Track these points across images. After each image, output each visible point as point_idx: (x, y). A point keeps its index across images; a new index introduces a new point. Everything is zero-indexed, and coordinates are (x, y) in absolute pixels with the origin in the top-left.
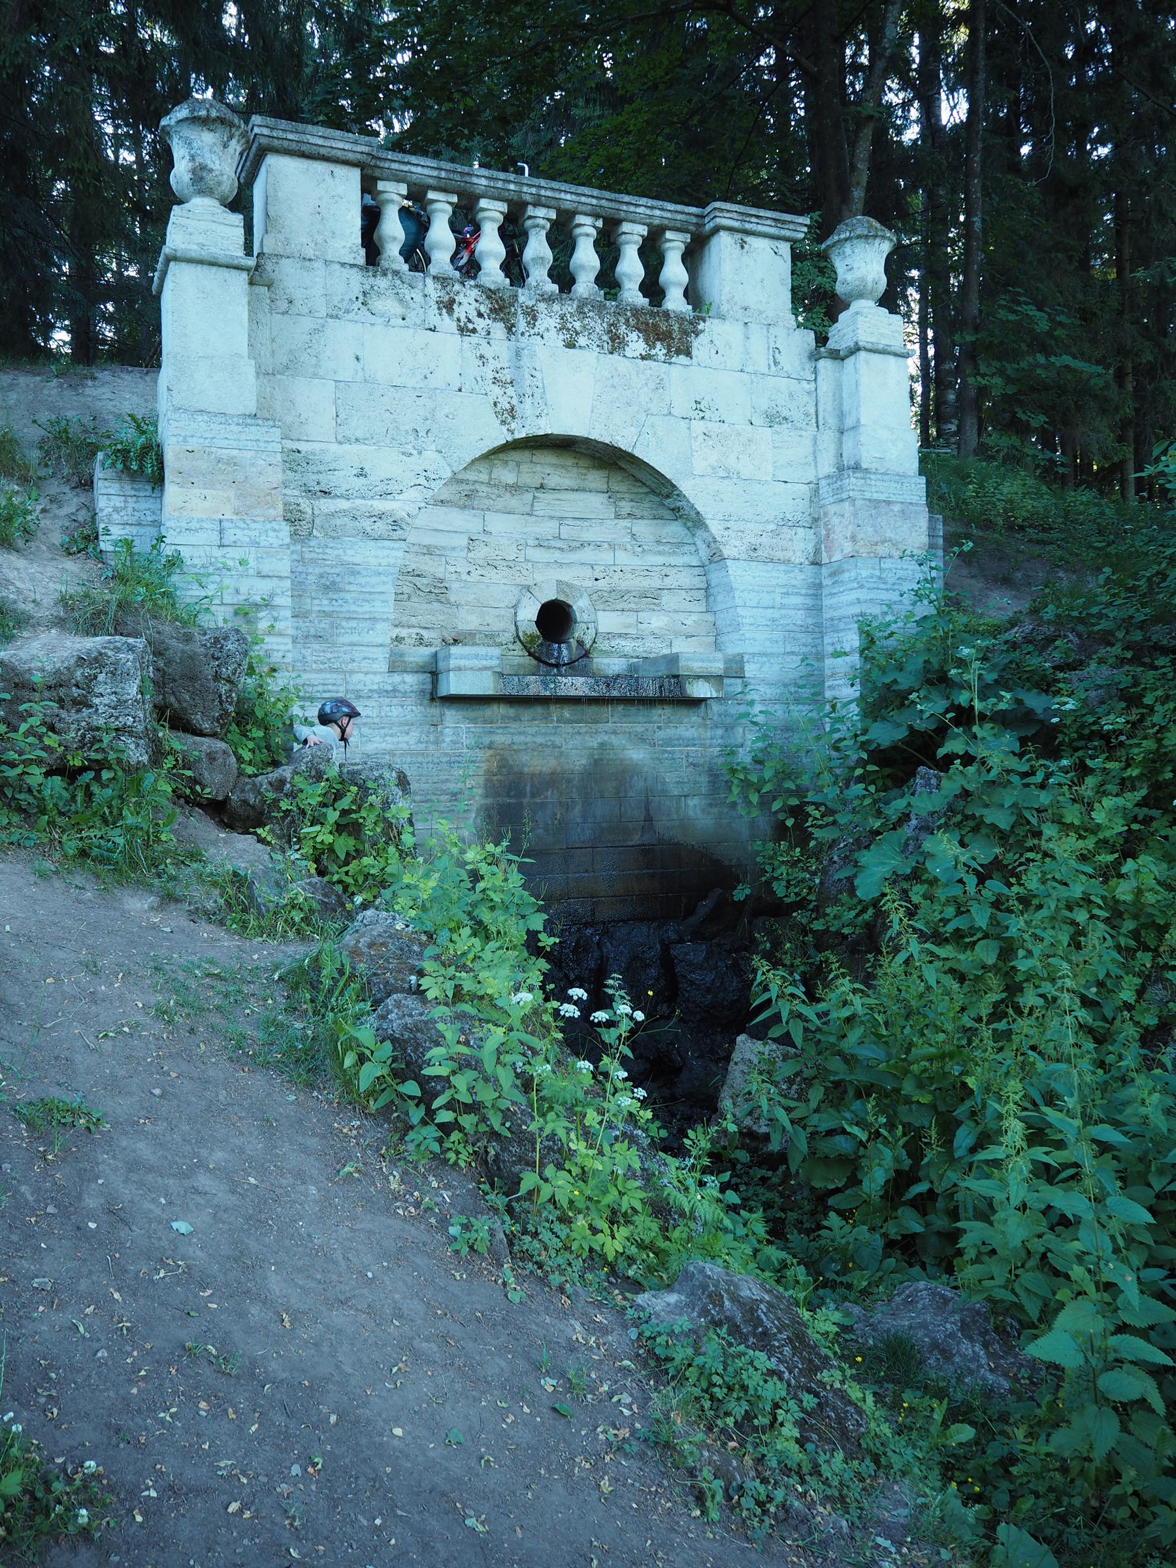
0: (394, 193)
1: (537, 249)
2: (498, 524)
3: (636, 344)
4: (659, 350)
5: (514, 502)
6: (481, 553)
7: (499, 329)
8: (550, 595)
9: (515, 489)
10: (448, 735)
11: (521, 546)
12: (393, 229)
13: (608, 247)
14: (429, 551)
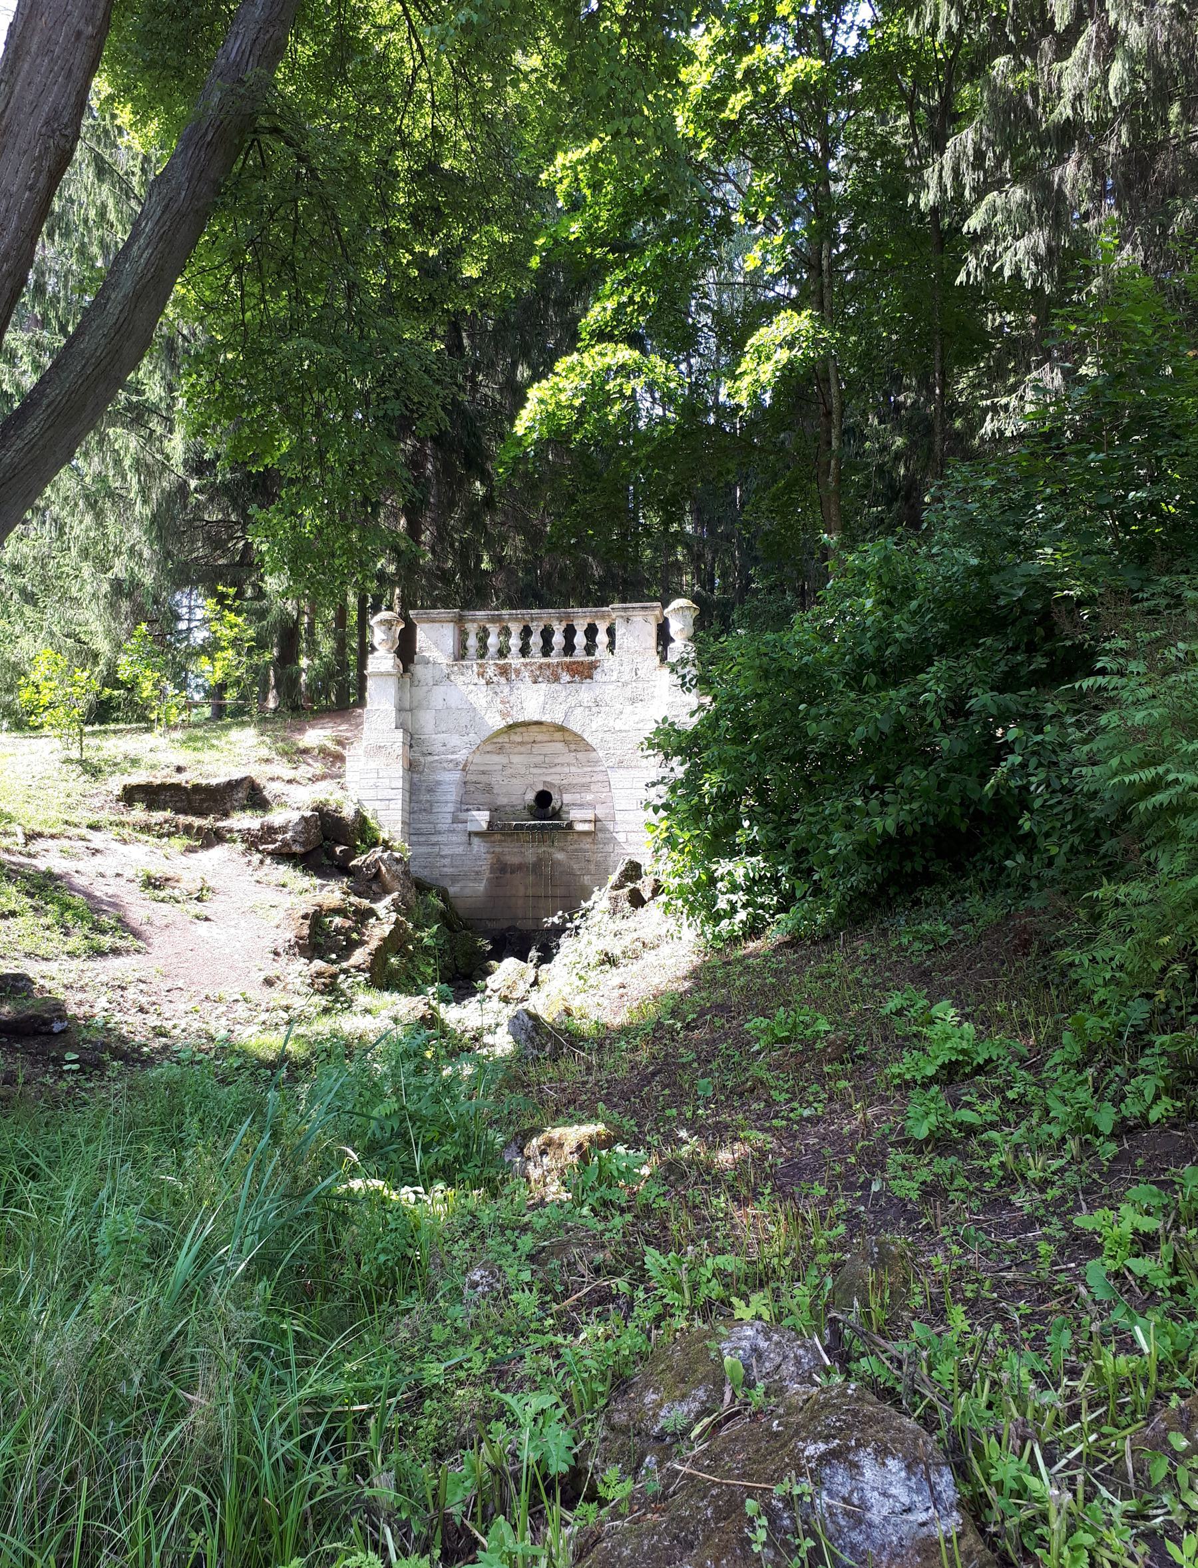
0: (472, 628)
1: (536, 640)
2: (516, 759)
3: (566, 677)
4: (577, 678)
5: (522, 749)
6: (509, 771)
7: (503, 680)
8: (540, 788)
9: (522, 743)
10: (475, 848)
11: (528, 767)
12: (472, 642)
13: (570, 632)
14: (483, 773)
